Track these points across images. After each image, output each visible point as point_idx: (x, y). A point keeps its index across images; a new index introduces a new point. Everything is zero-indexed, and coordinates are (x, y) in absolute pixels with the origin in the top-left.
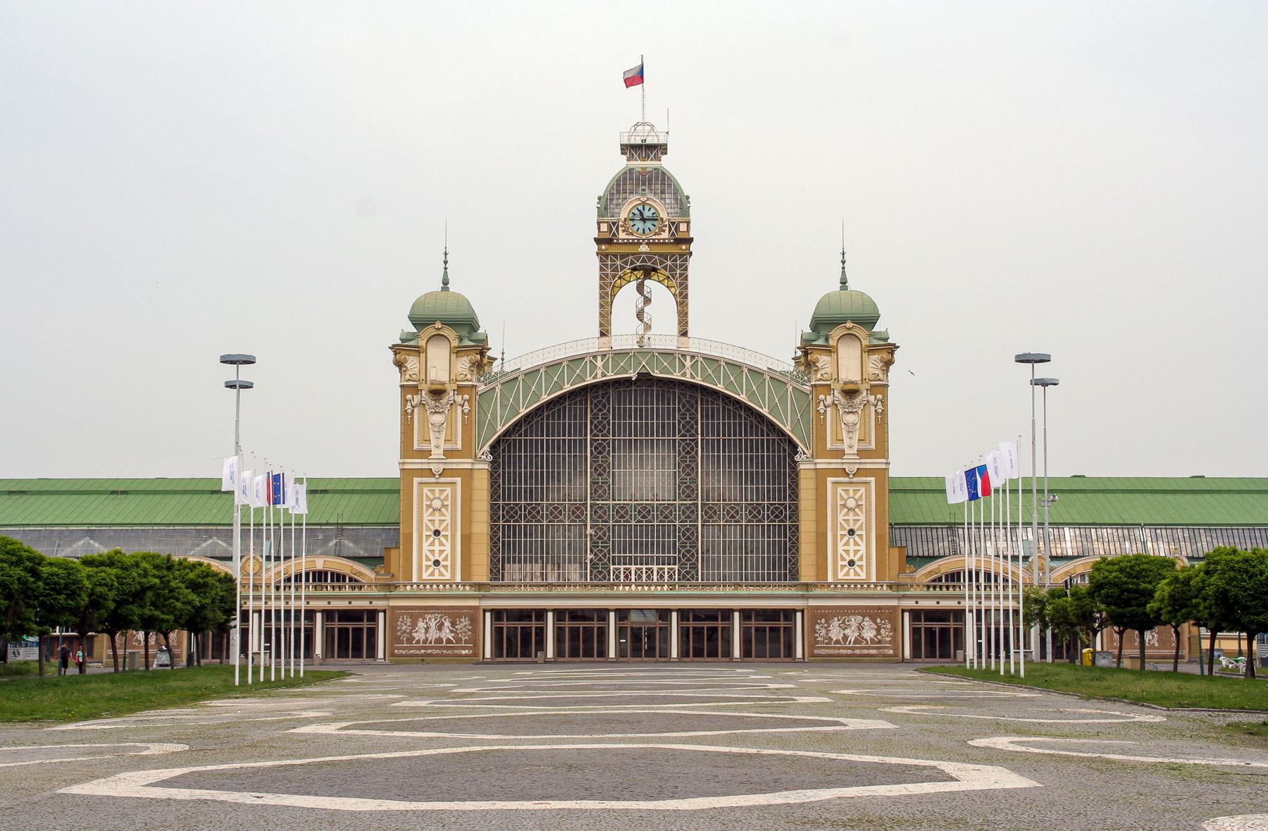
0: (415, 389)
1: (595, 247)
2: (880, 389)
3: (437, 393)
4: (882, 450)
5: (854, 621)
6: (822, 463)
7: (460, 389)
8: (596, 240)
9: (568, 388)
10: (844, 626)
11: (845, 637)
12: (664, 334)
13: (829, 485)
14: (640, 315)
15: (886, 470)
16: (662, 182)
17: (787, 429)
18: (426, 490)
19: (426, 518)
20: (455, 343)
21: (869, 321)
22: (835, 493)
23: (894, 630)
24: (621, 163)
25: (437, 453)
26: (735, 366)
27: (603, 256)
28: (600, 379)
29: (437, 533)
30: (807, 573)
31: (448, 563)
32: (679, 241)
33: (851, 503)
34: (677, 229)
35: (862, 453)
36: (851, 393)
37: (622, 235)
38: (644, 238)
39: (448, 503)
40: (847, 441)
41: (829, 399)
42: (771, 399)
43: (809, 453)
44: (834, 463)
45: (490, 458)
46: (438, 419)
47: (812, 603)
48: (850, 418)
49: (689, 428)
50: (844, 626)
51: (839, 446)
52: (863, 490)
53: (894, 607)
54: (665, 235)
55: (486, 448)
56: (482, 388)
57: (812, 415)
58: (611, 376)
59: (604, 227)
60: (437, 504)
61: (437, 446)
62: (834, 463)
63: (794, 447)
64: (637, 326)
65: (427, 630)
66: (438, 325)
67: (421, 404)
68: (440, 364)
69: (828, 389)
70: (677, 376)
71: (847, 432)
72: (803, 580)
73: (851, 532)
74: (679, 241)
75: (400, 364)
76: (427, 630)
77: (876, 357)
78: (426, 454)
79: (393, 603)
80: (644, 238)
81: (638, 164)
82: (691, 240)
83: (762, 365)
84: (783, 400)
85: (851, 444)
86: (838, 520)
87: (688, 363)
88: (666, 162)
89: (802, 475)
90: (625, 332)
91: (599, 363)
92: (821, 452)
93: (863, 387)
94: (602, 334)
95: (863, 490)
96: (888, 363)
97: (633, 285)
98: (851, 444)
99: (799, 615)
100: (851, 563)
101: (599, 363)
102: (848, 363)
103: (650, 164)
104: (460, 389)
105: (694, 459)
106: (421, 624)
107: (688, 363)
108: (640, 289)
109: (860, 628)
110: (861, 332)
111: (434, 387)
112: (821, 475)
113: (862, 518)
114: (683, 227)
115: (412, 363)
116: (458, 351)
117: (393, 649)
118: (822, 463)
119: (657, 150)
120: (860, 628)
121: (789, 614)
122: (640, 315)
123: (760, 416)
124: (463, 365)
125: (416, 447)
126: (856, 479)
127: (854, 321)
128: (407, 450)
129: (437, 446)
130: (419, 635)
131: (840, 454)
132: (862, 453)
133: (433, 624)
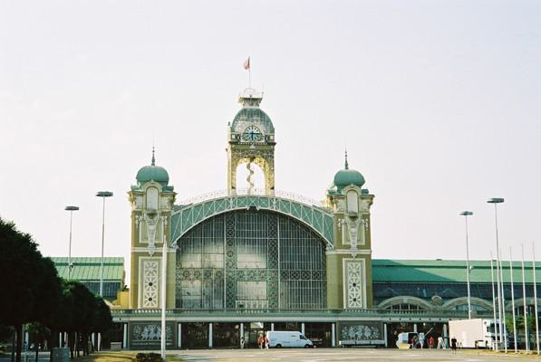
0: (140, 213)
1: (228, 146)
2: (367, 216)
3: (152, 215)
4: (368, 245)
5: (360, 328)
6: (340, 252)
7: (163, 214)
8: (230, 143)
9: (216, 213)
10: (356, 330)
11: (356, 336)
12: (260, 189)
13: (344, 262)
14: (248, 180)
15: (370, 255)
16: (261, 114)
17: (322, 235)
18: (145, 263)
19: (145, 276)
20: (161, 191)
21: (360, 182)
22: (346, 266)
23: (380, 332)
24: (240, 107)
25: (151, 244)
26: (297, 205)
27: (233, 150)
28: (232, 209)
29: (151, 284)
30: (332, 302)
31: (156, 299)
32: (269, 144)
33: (355, 271)
34: (269, 138)
35: (359, 247)
36: (354, 218)
37: (242, 141)
38: (253, 143)
39: (157, 269)
40: (352, 241)
41: (343, 221)
42: (315, 220)
43: (333, 246)
44: (346, 252)
45: (177, 247)
46: (152, 228)
47: (340, 319)
48: (353, 230)
49: (274, 233)
50: (356, 330)
51: (348, 243)
52: (360, 264)
53: (379, 321)
54: (263, 141)
55: (175, 242)
56: (173, 213)
57: (334, 228)
58: (237, 208)
59: (234, 137)
60: (151, 269)
61: (151, 241)
62: (346, 252)
63: (324, 244)
64: (248, 185)
65: (149, 333)
66: (152, 181)
67: (143, 220)
68: (154, 199)
69: (342, 216)
70: (269, 208)
71: (351, 234)
72: (329, 307)
73: (354, 285)
74: (269, 144)
75: (132, 200)
76: (149, 333)
77: (365, 201)
78: (146, 245)
79: (132, 319)
80: (253, 143)
81: (248, 107)
82: (274, 144)
83: (310, 204)
84: (320, 222)
85: (353, 243)
86: (348, 279)
87: (274, 203)
88: (262, 107)
89: (328, 258)
90: (242, 189)
91: (231, 202)
92: (340, 246)
93: (360, 215)
94: (233, 188)
95: (360, 264)
96: (371, 204)
97: (245, 164)
98: (353, 243)
99: (333, 325)
100: (355, 300)
101: (231, 202)
102: (353, 202)
103: (254, 107)
104: (163, 214)
105: (276, 249)
106: (146, 330)
107: (274, 203)
108: (248, 167)
109: (363, 332)
110: (356, 188)
111: (150, 212)
112: (340, 257)
113: (359, 278)
114: (271, 138)
115: (140, 199)
116: (162, 195)
117: (131, 342)
118: (340, 252)
119: (256, 101)
120: (363, 332)
121: (328, 325)
122: (248, 180)
123: (308, 229)
124: (166, 200)
125: (140, 241)
126: (357, 259)
127: (354, 184)
128: (136, 243)
129: (151, 241)
130: (145, 335)
131: (349, 247)
132: (359, 247)
133: (152, 330)
